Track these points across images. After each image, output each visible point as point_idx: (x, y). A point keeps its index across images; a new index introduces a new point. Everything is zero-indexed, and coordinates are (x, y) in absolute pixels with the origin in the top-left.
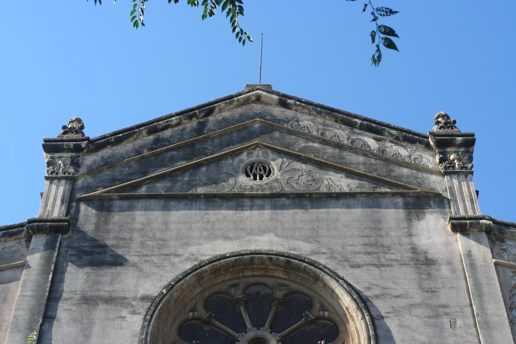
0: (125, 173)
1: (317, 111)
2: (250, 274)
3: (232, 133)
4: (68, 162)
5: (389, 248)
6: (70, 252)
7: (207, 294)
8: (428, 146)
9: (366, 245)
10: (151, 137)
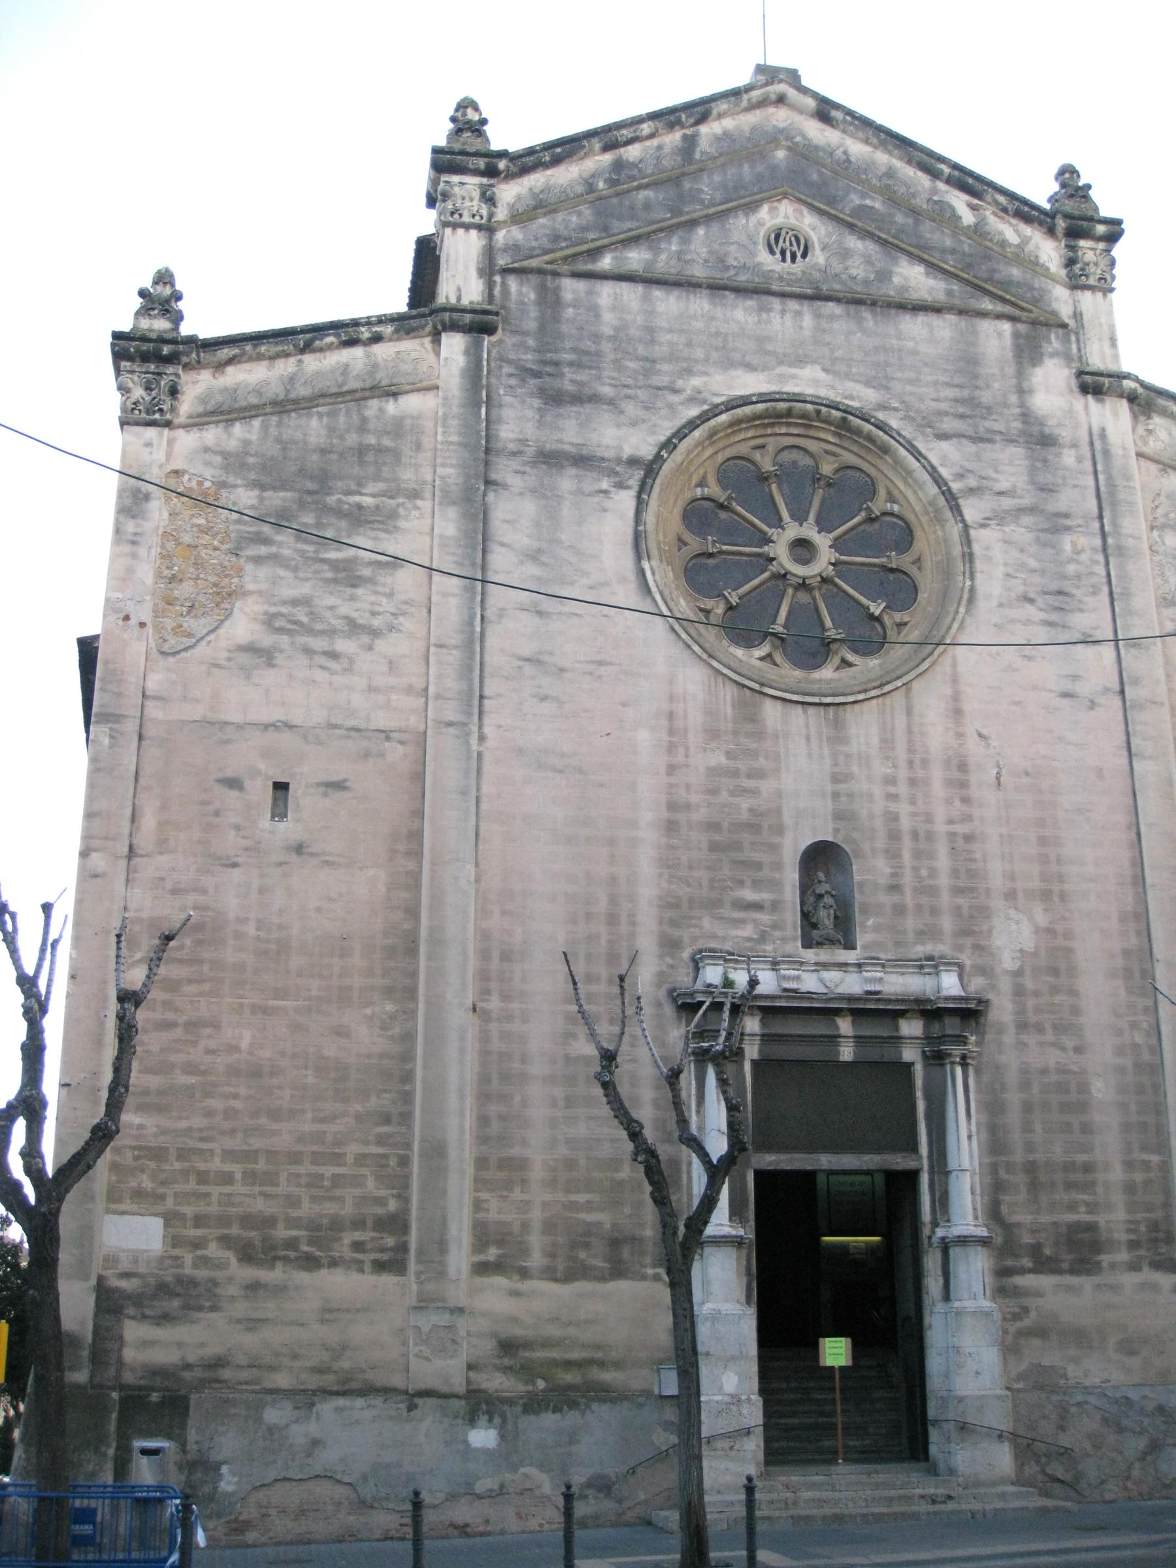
0: (573, 226)
1: (880, 140)
2: (783, 430)
3: (741, 166)
4: (476, 194)
5: (989, 409)
6: (507, 369)
7: (720, 458)
8: (1051, 232)
9: (956, 400)
10: (608, 158)
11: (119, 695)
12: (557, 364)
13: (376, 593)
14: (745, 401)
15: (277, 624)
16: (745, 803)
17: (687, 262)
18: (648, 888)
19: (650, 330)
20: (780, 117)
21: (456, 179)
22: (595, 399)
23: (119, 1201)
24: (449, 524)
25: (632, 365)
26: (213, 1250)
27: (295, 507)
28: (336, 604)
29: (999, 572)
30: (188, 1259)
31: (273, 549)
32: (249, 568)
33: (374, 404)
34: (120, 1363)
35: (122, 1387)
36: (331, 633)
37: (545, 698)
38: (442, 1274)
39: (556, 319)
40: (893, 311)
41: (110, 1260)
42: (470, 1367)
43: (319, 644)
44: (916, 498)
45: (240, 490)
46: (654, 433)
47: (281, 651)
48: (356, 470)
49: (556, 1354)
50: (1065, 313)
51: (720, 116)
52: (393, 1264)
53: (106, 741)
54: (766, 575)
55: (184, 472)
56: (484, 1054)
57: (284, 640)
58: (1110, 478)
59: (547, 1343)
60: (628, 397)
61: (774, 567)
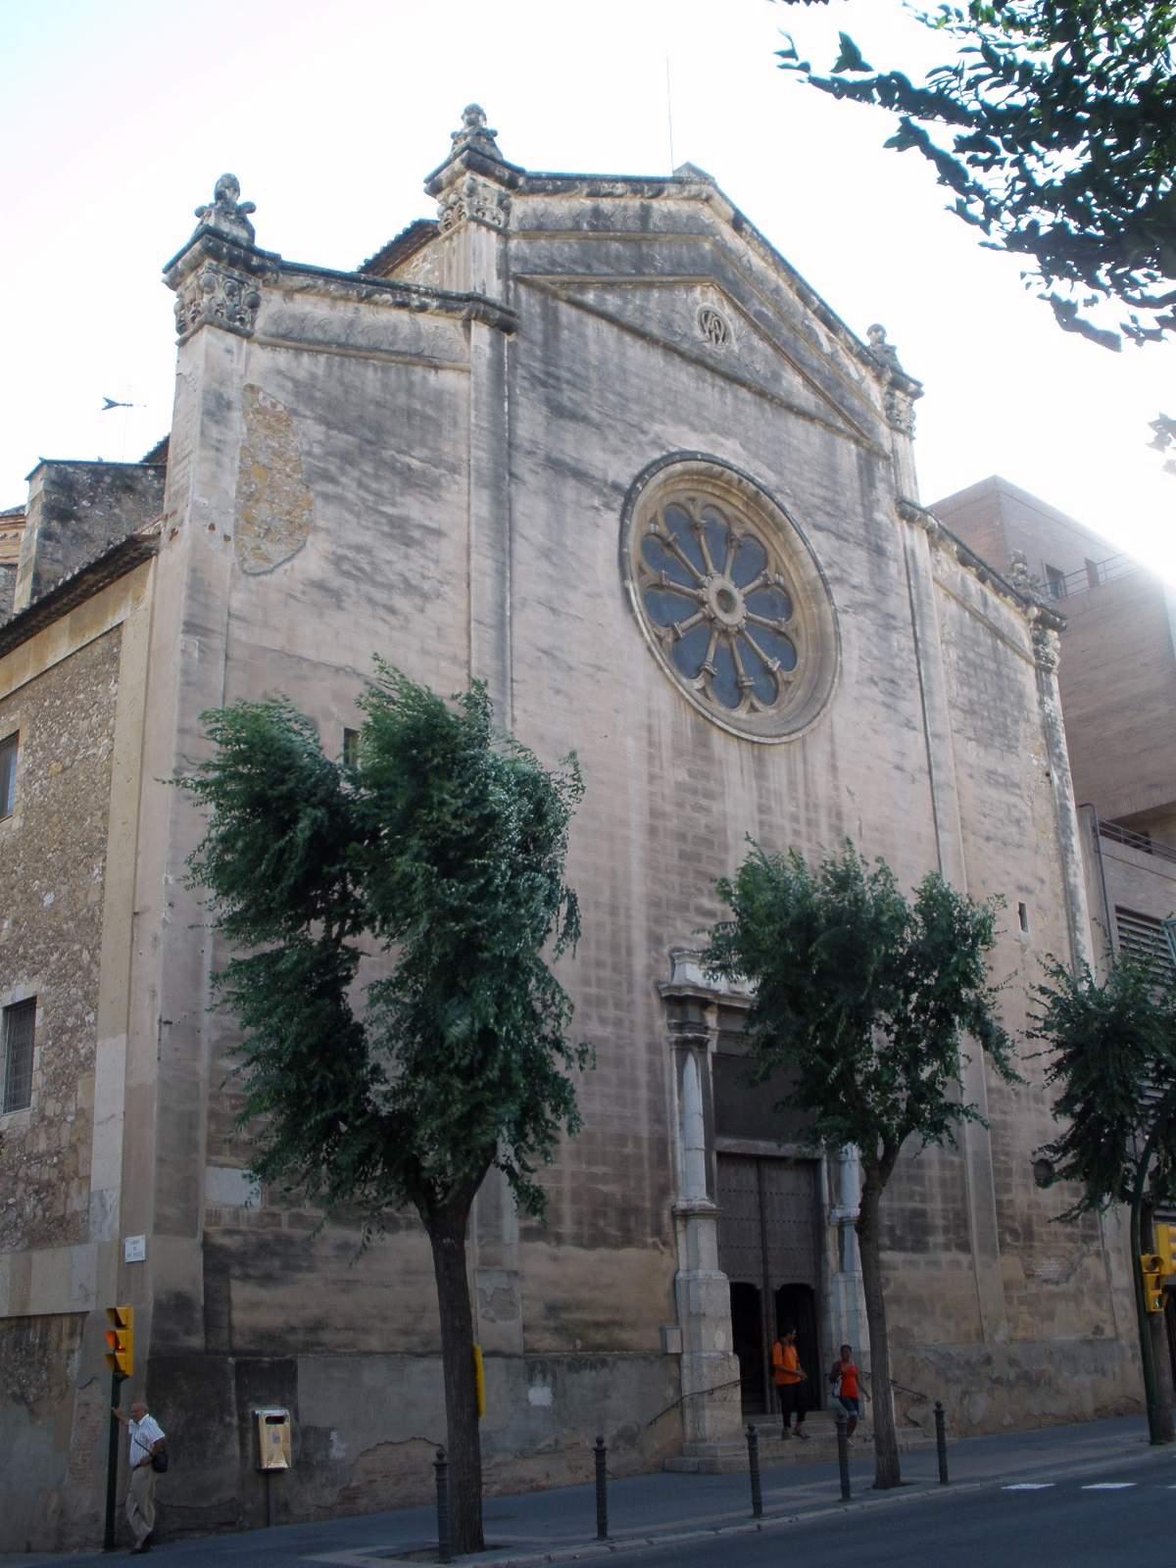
2: (710, 490)
9: (825, 499)
10: (588, 203)
11: (206, 606)
12: (558, 379)
13: (425, 557)
14: (691, 456)
15: (346, 567)
16: (703, 820)
17: (647, 318)
18: (638, 887)
19: (624, 371)
20: (706, 214)
21: (481, 179)
22: (585, 419)
23: (218, 1153)
24: (482, 505)
25: (611, 397)
27: (357, 452)
28: (393, 559)
29: (856, 653)
30: (285, 1217)
31: (339, 490)
32: (319, 503)
34: (231, 1327)
35: (234, 1353)
36: (389, 587)
37: (558, 692)
38: (498, 1238)
39: (556, 337)
40: (783, 411)
41: (214, 1216)
42: (525, 1328)
43: (380, 596)
44: (798, 576)
45: (309, 421)
46: (629, 465)
47: (348, 595)
48: (406, 431)
49: (587, 1316)
50: (887, 447)
51: (669, 197)
53: (196, 654)
54: (699, 616)
55: (259, 390)
57: (351, 584)
58: (918, 594)
59: (579, 1306)
60: (610, 426)
61: (705, 610)
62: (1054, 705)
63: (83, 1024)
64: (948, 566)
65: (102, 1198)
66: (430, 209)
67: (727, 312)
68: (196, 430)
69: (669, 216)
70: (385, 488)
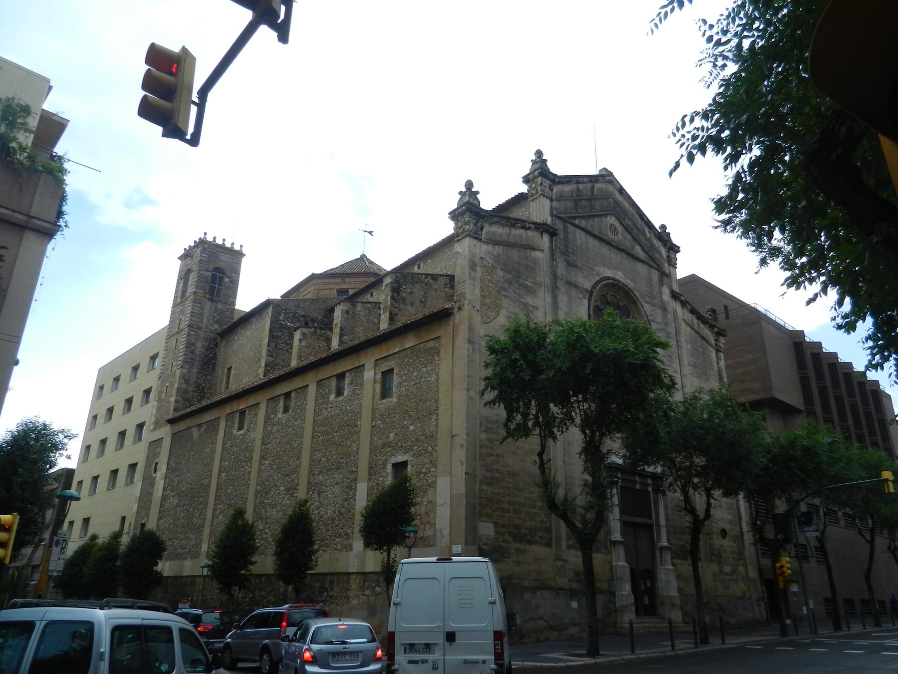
20: (611, 188)
24: (549, 299)
26: (507, 537)
33: (529, 251)
50: (667, 271)
52: (548, 544)
56: (565, 475)
62: (722, 363)
63: (430, 471)
64: (688, 316)
65: (441, 530)
66: (524, 188)
67: (617, 224)
68: (467, 274)
69: (600, 189)
70: (521, 293)
